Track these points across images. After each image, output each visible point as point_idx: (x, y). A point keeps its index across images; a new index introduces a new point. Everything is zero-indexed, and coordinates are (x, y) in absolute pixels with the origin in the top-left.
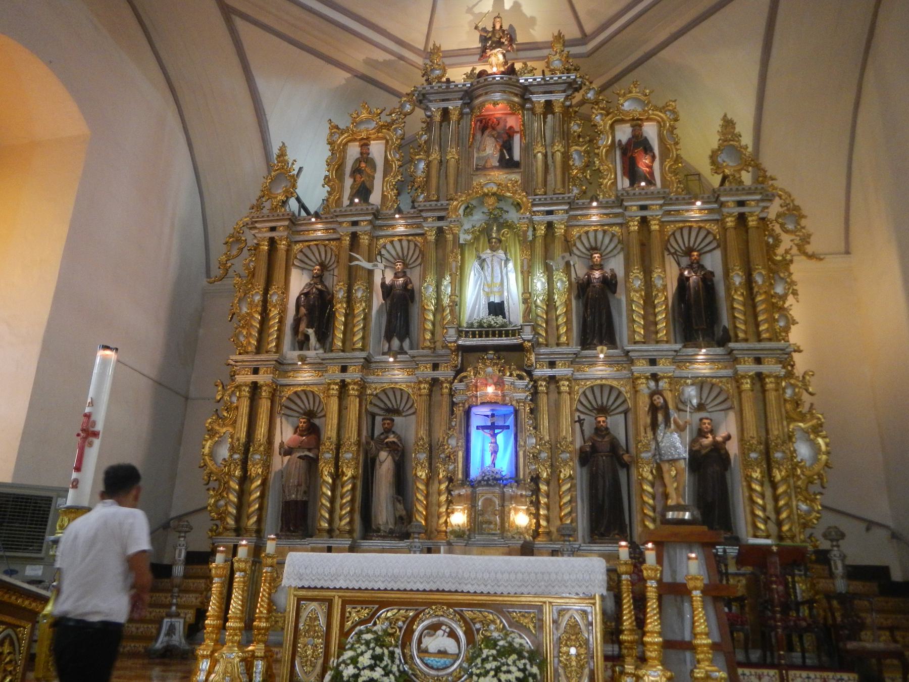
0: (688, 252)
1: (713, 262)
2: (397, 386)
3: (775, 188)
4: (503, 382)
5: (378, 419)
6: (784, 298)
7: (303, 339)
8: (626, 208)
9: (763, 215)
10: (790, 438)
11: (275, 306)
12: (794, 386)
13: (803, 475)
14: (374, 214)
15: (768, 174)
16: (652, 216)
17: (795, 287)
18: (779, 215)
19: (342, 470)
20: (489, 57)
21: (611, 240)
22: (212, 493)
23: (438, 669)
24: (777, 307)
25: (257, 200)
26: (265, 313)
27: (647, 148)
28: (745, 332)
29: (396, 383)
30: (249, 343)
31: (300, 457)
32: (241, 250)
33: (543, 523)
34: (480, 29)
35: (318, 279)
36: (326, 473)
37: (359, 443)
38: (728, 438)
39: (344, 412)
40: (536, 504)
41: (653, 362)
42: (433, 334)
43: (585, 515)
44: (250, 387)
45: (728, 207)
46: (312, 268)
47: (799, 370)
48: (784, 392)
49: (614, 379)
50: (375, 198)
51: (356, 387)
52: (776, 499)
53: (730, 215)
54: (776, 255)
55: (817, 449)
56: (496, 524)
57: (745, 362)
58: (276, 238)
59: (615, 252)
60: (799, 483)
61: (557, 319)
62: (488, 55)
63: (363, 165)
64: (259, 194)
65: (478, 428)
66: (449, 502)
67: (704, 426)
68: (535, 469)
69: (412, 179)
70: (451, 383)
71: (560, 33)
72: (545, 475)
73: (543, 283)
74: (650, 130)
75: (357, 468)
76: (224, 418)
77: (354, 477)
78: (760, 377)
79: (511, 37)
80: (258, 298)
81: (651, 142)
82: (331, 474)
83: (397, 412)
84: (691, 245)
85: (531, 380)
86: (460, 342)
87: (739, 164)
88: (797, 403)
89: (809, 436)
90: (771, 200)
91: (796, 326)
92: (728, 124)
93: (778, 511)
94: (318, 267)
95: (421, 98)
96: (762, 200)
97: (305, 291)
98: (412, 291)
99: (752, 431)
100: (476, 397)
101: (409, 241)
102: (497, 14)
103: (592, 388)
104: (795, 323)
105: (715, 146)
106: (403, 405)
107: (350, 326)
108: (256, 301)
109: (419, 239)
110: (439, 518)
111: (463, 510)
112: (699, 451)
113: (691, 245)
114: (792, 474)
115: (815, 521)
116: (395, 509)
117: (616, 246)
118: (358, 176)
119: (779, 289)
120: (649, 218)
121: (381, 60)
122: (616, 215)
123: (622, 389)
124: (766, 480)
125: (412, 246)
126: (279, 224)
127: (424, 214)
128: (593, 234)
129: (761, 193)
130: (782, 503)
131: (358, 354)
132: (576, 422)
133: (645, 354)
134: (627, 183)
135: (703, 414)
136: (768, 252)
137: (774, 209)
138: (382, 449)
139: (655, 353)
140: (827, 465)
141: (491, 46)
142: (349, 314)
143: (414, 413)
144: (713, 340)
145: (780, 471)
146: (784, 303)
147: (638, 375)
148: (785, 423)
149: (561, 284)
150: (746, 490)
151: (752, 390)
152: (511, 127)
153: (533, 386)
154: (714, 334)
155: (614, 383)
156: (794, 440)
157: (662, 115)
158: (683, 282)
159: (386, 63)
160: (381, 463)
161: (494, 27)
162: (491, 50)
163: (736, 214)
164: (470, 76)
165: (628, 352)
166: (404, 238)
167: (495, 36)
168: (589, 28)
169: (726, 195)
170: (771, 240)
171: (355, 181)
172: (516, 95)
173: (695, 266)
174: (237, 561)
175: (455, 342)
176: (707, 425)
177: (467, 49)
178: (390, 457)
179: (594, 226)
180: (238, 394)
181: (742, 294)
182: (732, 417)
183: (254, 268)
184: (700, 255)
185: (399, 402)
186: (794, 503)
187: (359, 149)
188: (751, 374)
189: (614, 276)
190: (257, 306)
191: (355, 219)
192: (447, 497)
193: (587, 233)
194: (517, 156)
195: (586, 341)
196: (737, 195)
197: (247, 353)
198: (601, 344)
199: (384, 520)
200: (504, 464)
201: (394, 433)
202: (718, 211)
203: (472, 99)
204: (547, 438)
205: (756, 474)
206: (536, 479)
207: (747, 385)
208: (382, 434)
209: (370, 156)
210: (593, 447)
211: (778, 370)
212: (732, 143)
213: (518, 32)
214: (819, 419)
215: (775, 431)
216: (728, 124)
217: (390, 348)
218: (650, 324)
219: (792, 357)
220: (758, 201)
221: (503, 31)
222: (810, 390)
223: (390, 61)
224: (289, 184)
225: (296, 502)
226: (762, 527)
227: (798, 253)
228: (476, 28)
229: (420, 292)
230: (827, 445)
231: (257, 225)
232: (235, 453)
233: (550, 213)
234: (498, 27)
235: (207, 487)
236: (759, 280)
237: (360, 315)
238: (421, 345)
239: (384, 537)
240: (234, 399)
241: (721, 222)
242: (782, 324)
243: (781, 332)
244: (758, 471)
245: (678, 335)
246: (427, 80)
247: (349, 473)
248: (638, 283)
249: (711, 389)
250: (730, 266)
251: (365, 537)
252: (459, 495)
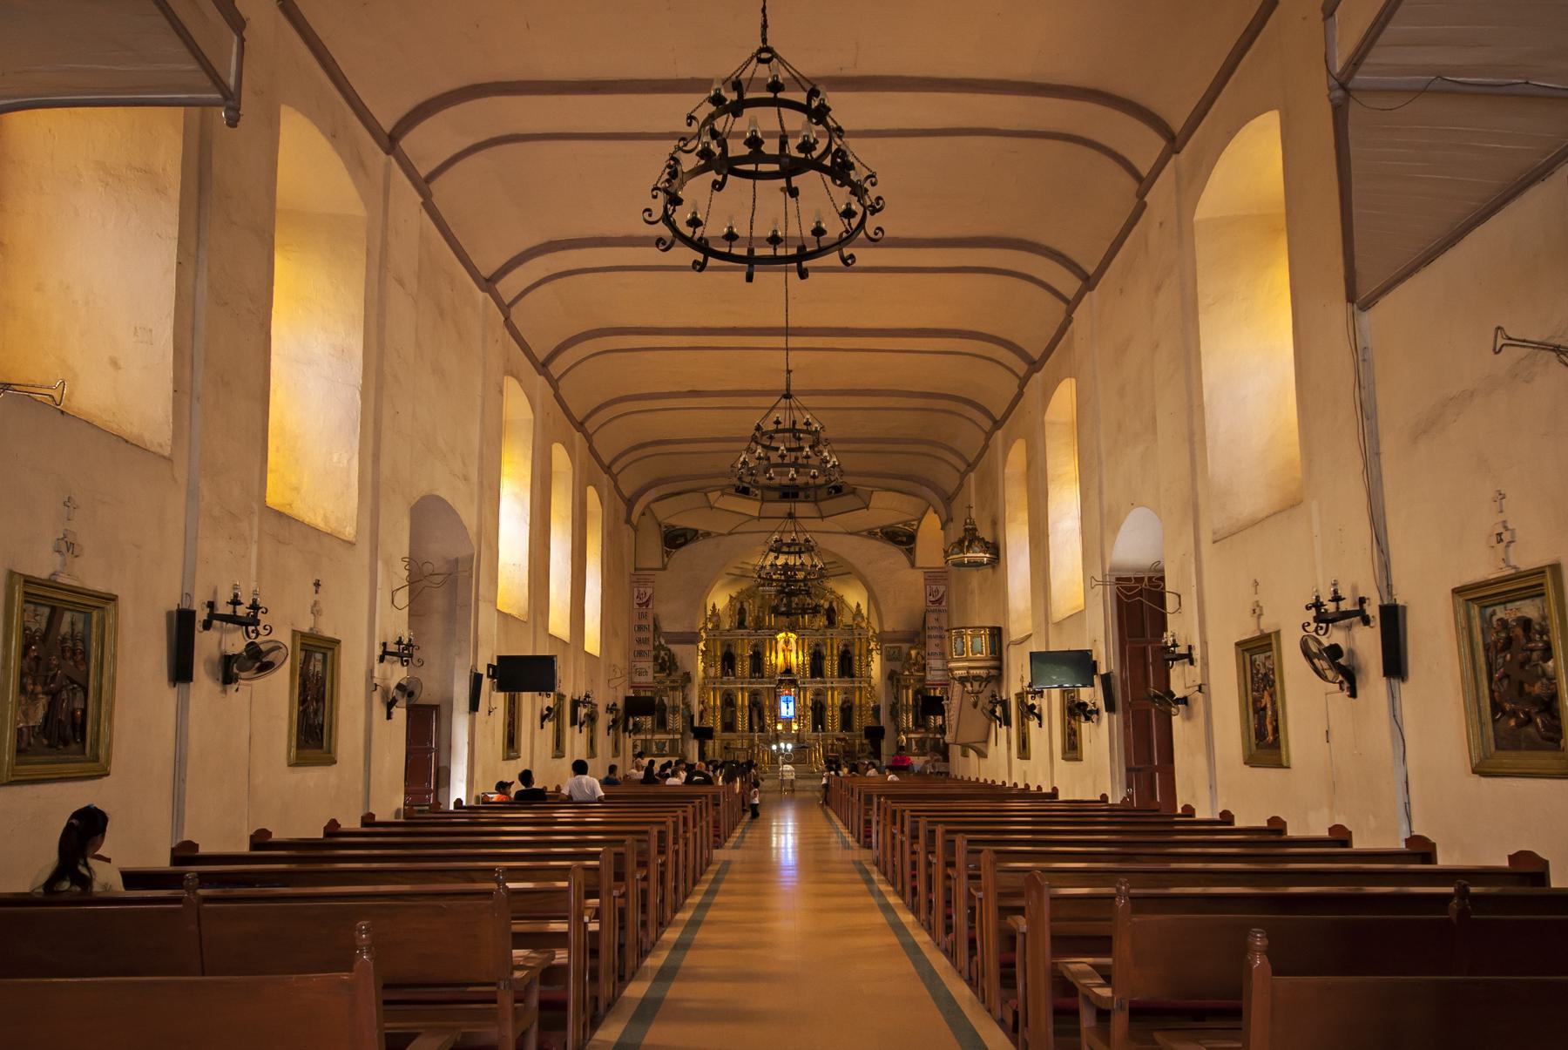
24: (868, 665)
47: (873, 684)
50: (746, 623)
74: (835, 604)
83: (757, 694)
92: (858, 605)
142: (742, 665)
195: (813, 676)
200: (791, 713)
211: (866, 685)
215: (863, 702)
216: (858, 605)
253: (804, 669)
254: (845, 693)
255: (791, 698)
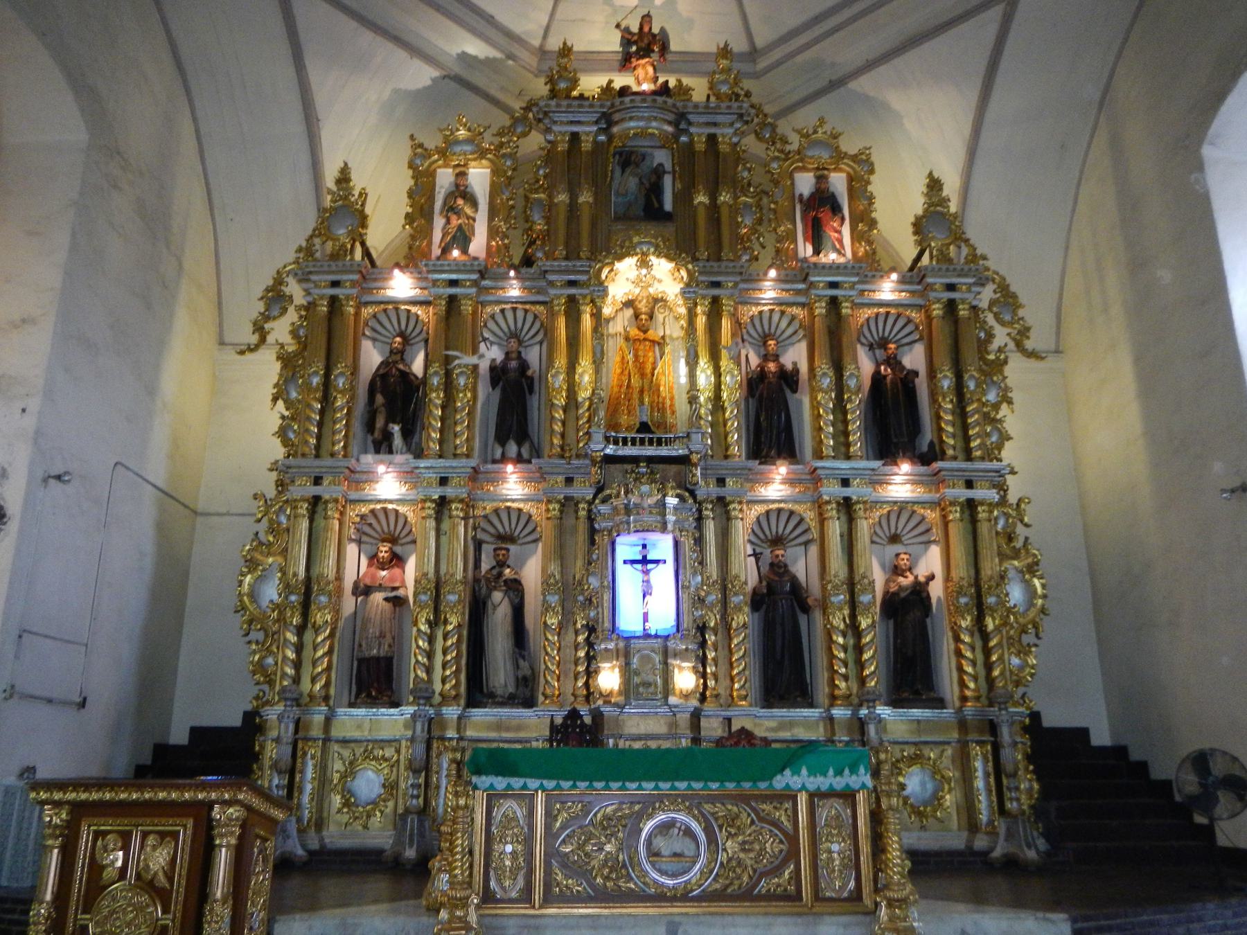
0: (883, 343)
1: (914, 359)
2: (515, 505)
3: (987, 269)
4: (664, 505)
5: (487, 550)
6: (996, 407)
7: (380, 437)
8: (812, 285)
9: (974, 303)
10: (1002, 577)
11: (342, 392)
12: (1007, 515)
13: (1017, 623)
14: (480, 272)
15: (979, 252)
16: (844, 296)
17: (1010, 395)
18: (992, 303)
19: (445, 617)
20: (635, 68)
21: (789, 324)
22: (254, 647)
23: (674, 875)
25: (308, 241)
26: (326, 399)
27: (836, 209)
28: (954, 448)
29: (513, 501)
30: (306, 442)
31: (386, 599)
32: (284, 311)
33: (711, 683)
34: (623, 27)
35: (399, 355)
36: (423, 620)
37: (464, 582)
38: (931, 577)
39: (444, 539)
40: (703, 661)
41: (845, 483)
42: (563, 436)
43: (757, 673)
44: (309, 504)
45: (935, 290)
46: (390, 341)
47: (1012, 498)
48: (996, 523)
49: (795, 502)
50: (478, 245)
51: (460, 506)
52: (987, 652)
53: (938, 301)
54: (988, 353)
55: (1031, 593)
56: (656, 686)
57: (954, 485)
58: (341, 297)
59: (795, 338)
60: (1012, 632)
61: (725, 425)
62: (633, 65)
63: (460, 202)
64: (310, 232)
65: (625, 562)
66: (590, 658)
67: (902, 563)
68: (702, 615)
69: (527, 226)
70: (591, 503)
71: (726, 45)
72: (712, 624)
73: (707, 377)
74: (838, 182)
75: (463, 613)
76: (270, 545)
77: (459, 625)
78: (971, 505)
79: (663, 44)
80: (316, 380)
81: (840, 200)
82: (428, 622)
83: (511, 539)
84: (886, 334)
85: (695, 501)
86: (608, 451)
87: (947, 237)
88: (1010, 538)
89: (1024, 576)
90: (983, 285)
91: (1010, 442)
92: (934, 185)
93: (989, 667)
94: (398, 339)
95: (541, 116)
96: (975, 284)
97: (382, 371)
98: (531, 379)
99: (961, 571)
100: (628, 523)
101: (526, 311)
102: (646, 13)
103: (768, 512)
104: (1009, 438)
105: (920, 212)
106: (519, 529)
107: (448, 422)
108: (314, 384)
109: (541, 308)
110: (576, 679)
111: (613, 668)
112: (895, 594)
113: (886, 334)
114: (1005, 623)
115: (1029, 679)
116: (517, 667)
117: (795, 332)
118: (454, 218)
119: (992, 396)
120: (841, 299)
121: (482, 56)
122: (798, 292)
123: (804, 515)
124: (975, 629)
125: (530, 318)
126: (345, 277)
127: (551, 277)
128: (768, 314)
129: (974, 276)
130: (994, 658)
131: (463, 462)
132: (750, 556)
133: (837, 472)
134: (810, 250)
135: (898, 548)
136: (979, 351)
137: (987, 294)
138: (495, 588)
139: (848, 472)
140: (1043, 611)
141: (637, 52)
143: (536, 541)
144: (914, 456)
145: (994, 619)
146: (997, 413)
147: (828, 498)
148: (997, 560)
149: (732, 380)
150: (951, 641)
151: (962, 520)
152: (661, 165)
153: (697, 510)
154: (915, 449)
155: (796, 508)
156: (1006, 581)
157: (856, 166)
158: (877, 379)
159: (488, 62)
160: (495, 607)
161: (641, 28)
162: (638, 60)
163: (945, 300)
164: (607, 90)
165: (815, 469)
166: (519, 306)
167: (642, 41)
168: (760, 42)
169: (935, 276)
170: (982, 335)
171: (448, 222)
172: (670, 123)
173: (892, 361)
174: (302, 739)
175: (603, 450)
176: (904, 561)
177: (599, 52)
178: (506, 599)
179: (771, 304)
180: (288, 512)
181: (951, 401)
182: (935, 552)
183: (306, 337)
184: (897, 349)
185: (513, 526)
186: (1006, 656)
187: (452, 179)
188: (961, 500)
189: (796, 371)
190: (316, 390)
191: (454, 276)
192: (587, 654)
193: (761, 313)
194: (668, 206)
196: (946, 277)
197: (304, 455)
198: (779, 456)
199: (502, 681)
201: (509, 567)
202: (922, 294)
203: (610, 124)
204: (715, 577)
205: (966, 622)
206: (702, 629)
207: (955, 514)
208: (493, 568)
209: (468, 190)
210: (769, 586)
211: (993, 495)
212: (938, 208)
213: (671, 37)
214: (1035, 555)
216: (934, 185)
217: (503, 454)
218: (842, 434)
219: (1005, 480)
220: (970, 285)
221: (654, 36)
222: (1026, 519)
223: (495, 59)
224: (356, 223)
225: (377, 659)
226: (972, 685)
227: (1015, 349)
228: (618, 26)
229: (543, 377)
230: (1043, 586)
231: (314, 277)
232: (291, 593)
233: (717, 285)
234: (646, 29)
235: (247, 639)
236: (972, 385)
237: (464, 409)
238: (546, 451)
239: (502, 704)
240: (283, 519)
241: (924, 308)
242: (994, 439)
243: (992, 449)
244: (969, 618)
245: (869, 448)
246: (552, 91)
247: (454, 620)
248: (826, 382)
249: (911, 516)
250: (937, 362)
251: (472, 702)
252: (606, 650)
253: (719, 426)
254: (895, 539)
255: (662, 546)
